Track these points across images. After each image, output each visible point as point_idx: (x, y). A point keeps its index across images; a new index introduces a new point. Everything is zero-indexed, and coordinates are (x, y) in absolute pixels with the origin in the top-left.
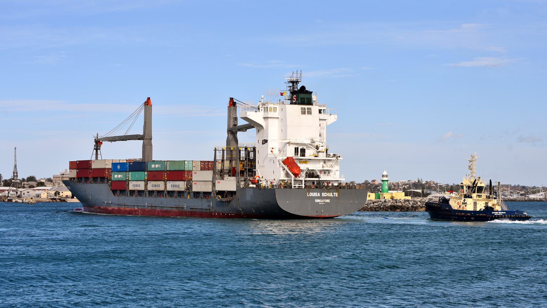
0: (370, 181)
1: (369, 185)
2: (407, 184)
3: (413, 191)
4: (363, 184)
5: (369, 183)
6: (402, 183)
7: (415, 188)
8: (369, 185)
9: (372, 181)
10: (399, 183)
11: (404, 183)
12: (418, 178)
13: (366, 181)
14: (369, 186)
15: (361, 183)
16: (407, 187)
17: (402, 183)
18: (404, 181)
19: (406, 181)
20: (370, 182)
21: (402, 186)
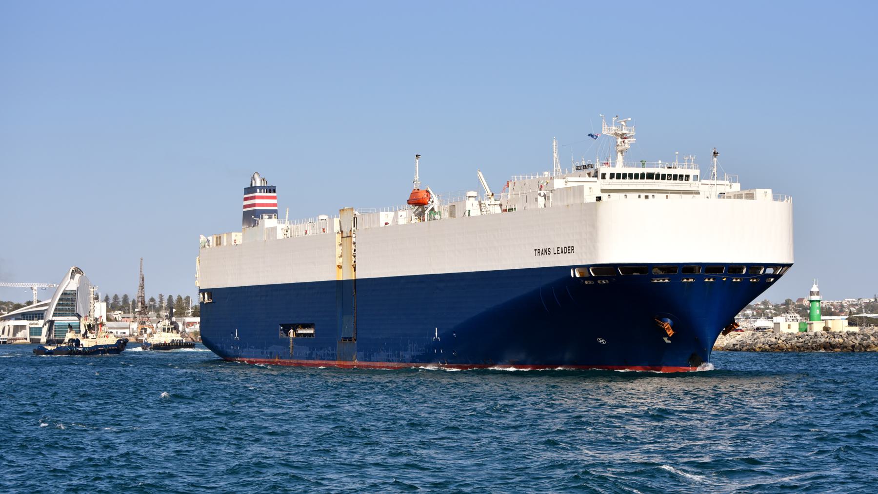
2: (857, 305)
3: (866, 317)
4: (782, 305)
7: (869, 312)
9: (797, 301)
10: (843, 303)
11: (851, 303)
12: (875, 295)
15: (779, 303)
16: (857, 309)
18: (852, 300)
19: (854, 300)
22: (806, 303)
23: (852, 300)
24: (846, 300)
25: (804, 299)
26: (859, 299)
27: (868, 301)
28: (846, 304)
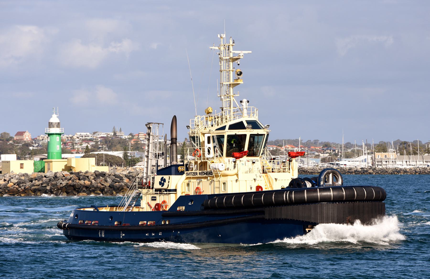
0: (12, 134)
1: (11, 142)
2: (91, 140)
3: (106, 155)
5: (11, 138)
6: (80, 138)
7: (107, 149)
8: (11, 142)
9: (16, 135)
10: (75, 137)
11: (84, 138)
13: (5, 133)
14: (11, 144)
16: (92, 146)
17: (80, 138)
18: (85, 134)
19: (88, 134)
20: (14, 136)
21: (81, 145)
22: (27, 137)
23: (85, 134)
24: (79, 134)
25: (24, 132)
26: (94, 133)
27: (105, 136)
28: (78, 139)
